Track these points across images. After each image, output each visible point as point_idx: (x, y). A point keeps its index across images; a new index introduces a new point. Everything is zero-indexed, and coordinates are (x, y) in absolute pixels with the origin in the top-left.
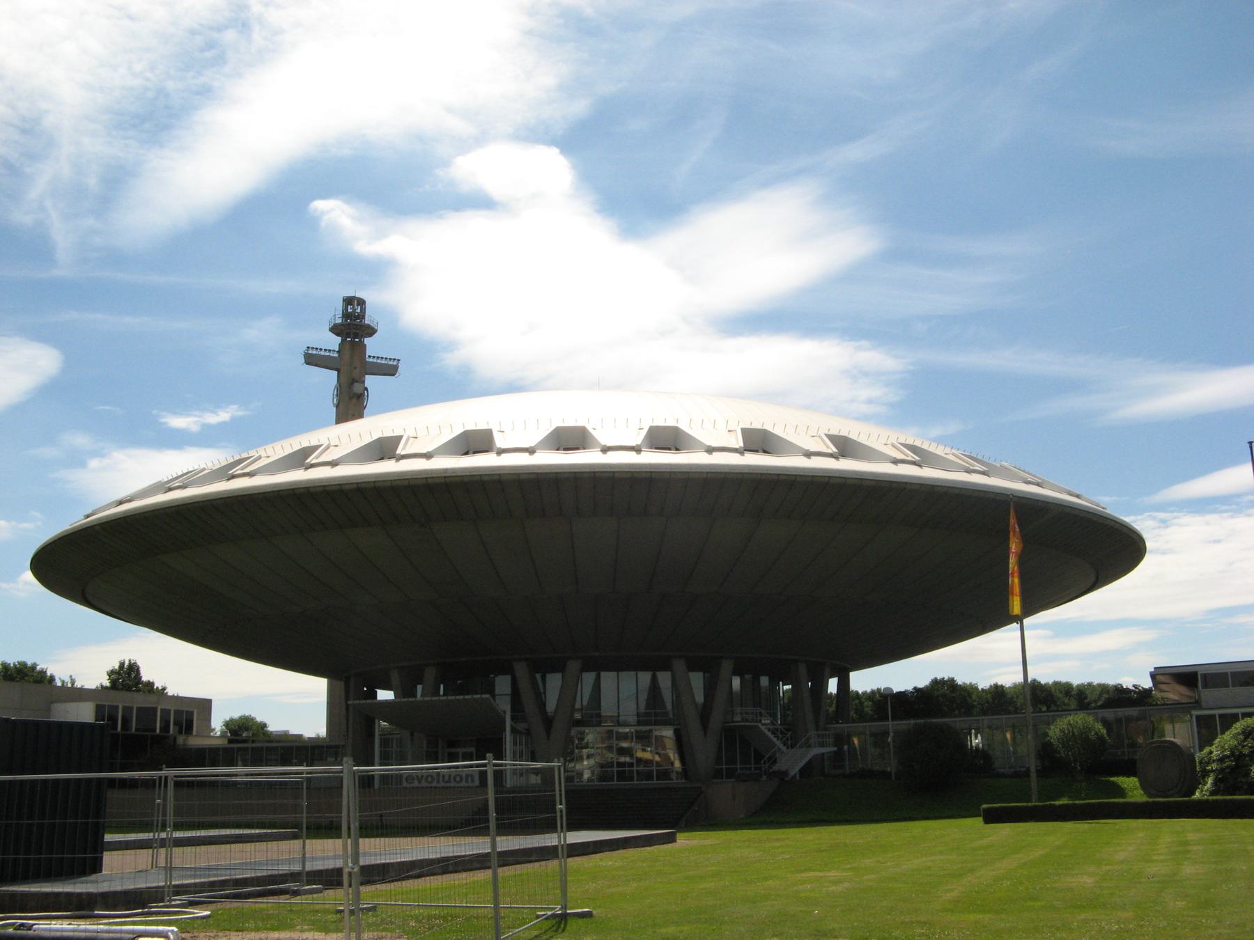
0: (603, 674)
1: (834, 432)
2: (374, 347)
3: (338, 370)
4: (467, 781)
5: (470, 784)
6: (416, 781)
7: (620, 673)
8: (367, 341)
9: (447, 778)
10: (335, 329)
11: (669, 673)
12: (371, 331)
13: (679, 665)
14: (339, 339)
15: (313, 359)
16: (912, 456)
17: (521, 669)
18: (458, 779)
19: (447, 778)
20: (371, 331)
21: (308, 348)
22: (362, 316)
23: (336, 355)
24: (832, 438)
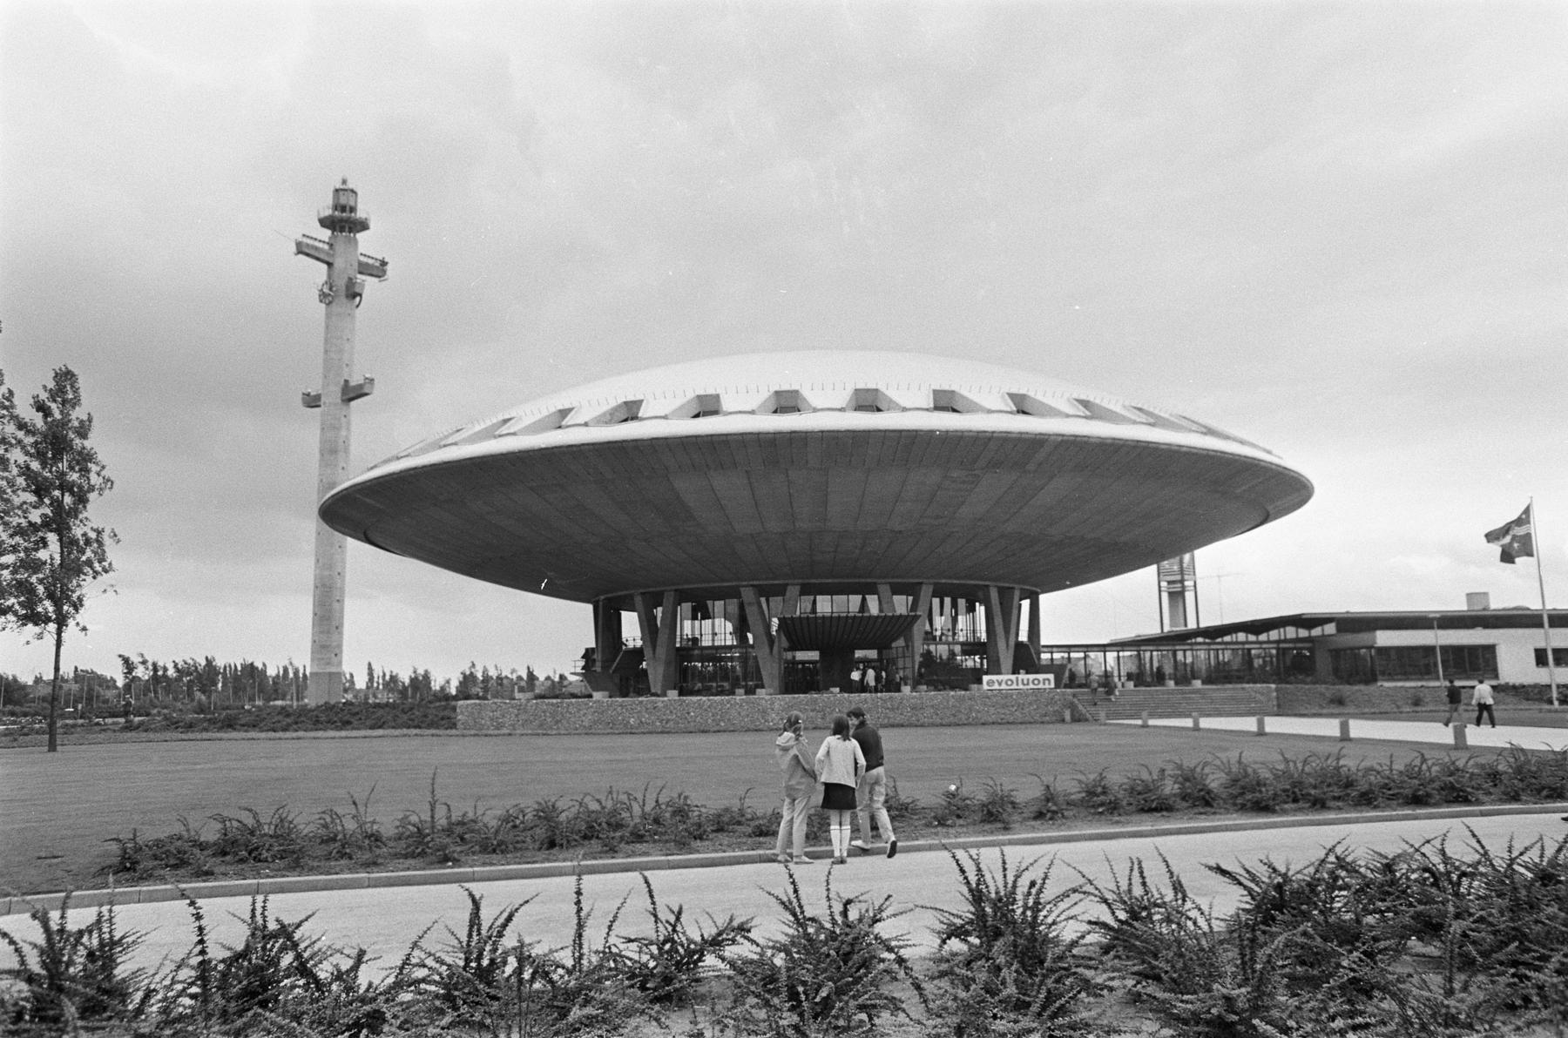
0: (818, 597)
1: (1014, 390)
2: (367, 244)
3: (330, 264)
4: (1044, 684)
5: (1047, 686)
6: (996, 684)
7: (834, 597)
8: (359, 236)
9: (1025, 682)
10: (325, 222)
11: (876, 597)
12: (363, 226)
13: (884, 589)
14: (329, 232)
15: (301, 250)
16: (1082, 411)
17: (748, 594)
18: (1036, 682)
19: (1025, 682)
20: (363, 226)
21: (304, 235)
22: (353, 209)
23: (326, 247)
24: (1012, 396)
